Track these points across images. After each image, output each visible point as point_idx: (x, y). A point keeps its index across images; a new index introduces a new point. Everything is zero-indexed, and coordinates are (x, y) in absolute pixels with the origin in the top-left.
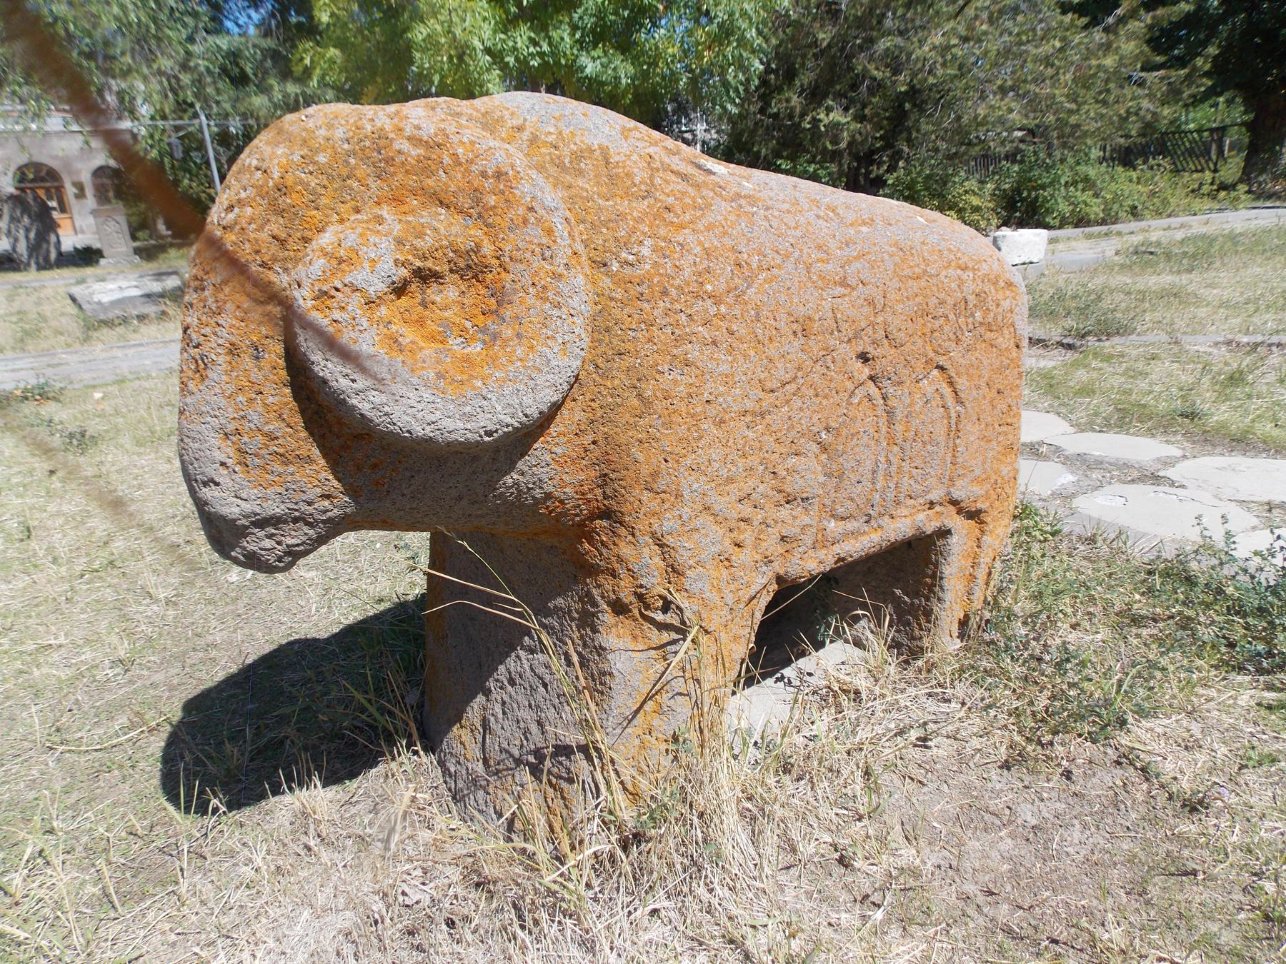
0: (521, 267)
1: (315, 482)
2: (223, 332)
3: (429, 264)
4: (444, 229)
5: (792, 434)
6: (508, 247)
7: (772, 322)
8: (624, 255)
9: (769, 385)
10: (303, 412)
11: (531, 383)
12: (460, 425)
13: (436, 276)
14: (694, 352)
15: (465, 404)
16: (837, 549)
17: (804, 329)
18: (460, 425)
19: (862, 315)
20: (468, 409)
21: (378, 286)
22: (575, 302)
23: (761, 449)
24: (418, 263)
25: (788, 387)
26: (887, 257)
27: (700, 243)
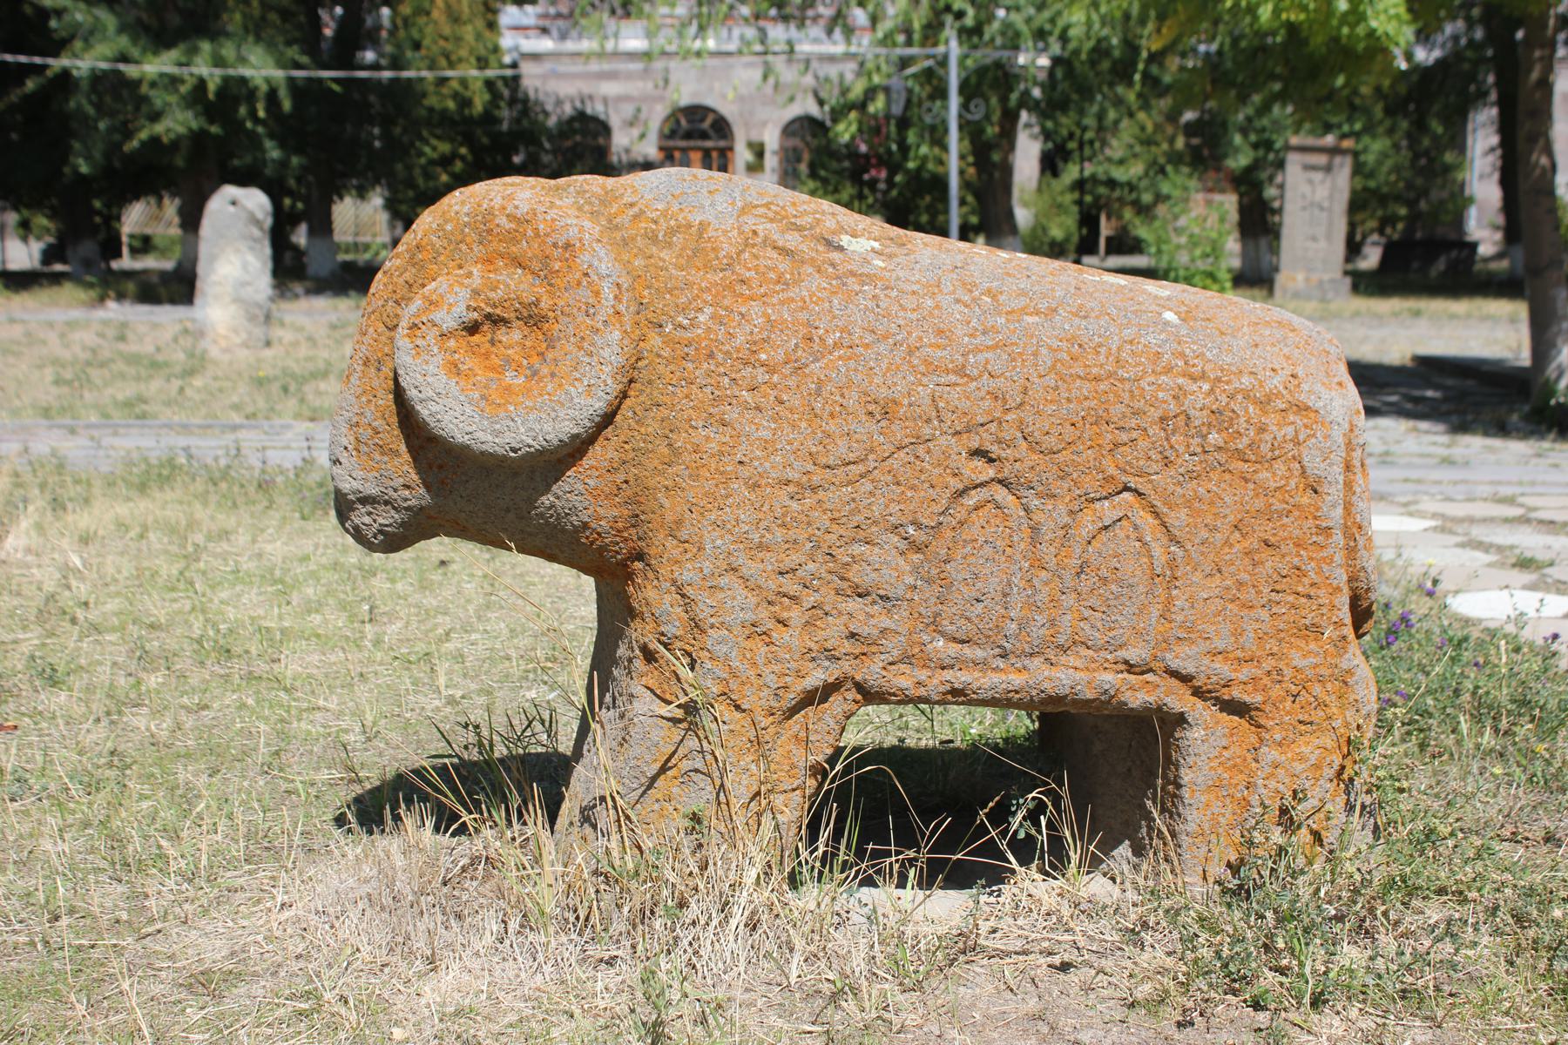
0: (567, 319)
1: (399, 475)
2: (363, 348)
3: (498, 311)
4: (514, 284)
6: (561, 303)
9: (824, 461)
10: (398, 414)
11: (553, 415)
12: (490, 438)
13: (505, 321)
14: (732, 414)
16: (948, 675)
17: (886, 411)
18: (490, 438)
19: (983, 409)
22: (606, 353)
23: (809, 524)
24: (489, 310)
26: (1044, 351)
27: (766, 315)
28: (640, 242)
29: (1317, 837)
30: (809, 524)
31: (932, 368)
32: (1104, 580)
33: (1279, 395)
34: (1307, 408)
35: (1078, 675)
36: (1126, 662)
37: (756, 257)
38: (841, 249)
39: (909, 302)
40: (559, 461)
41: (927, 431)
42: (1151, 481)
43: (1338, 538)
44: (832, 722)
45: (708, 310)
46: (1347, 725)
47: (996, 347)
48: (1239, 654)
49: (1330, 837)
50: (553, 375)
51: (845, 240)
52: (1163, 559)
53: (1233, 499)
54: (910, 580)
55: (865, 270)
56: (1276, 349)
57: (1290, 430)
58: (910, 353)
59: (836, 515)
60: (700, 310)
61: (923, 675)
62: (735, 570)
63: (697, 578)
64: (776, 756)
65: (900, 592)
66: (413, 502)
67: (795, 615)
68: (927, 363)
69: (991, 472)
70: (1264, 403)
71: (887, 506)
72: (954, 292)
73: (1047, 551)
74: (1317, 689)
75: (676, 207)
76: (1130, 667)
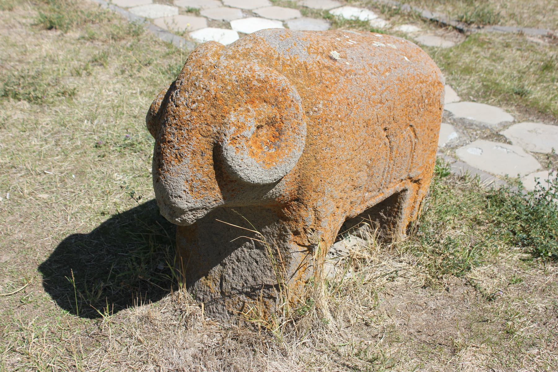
14: (334, 141)
20: (271, 173)
50: (286, 146)
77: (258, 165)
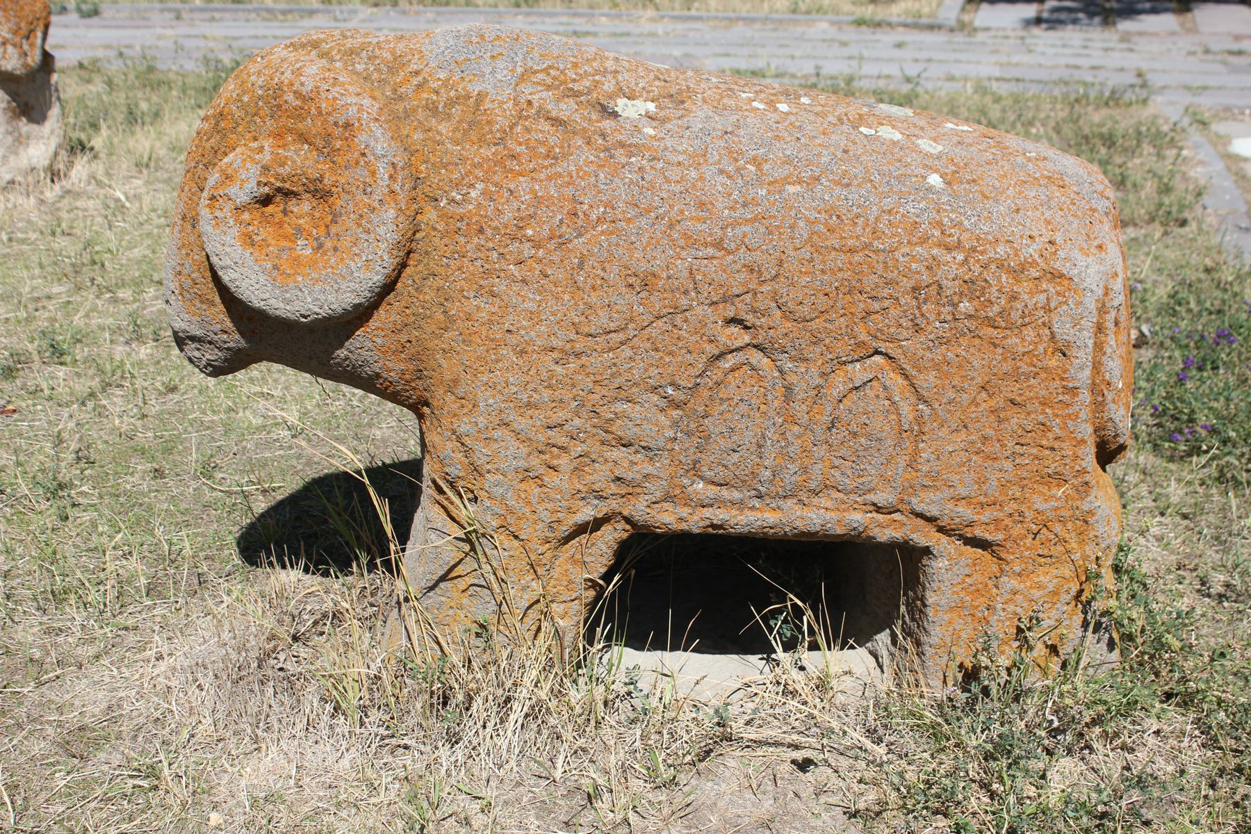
0: (347, 197)
3: (287, 186)
4: (300, 160)
5: (618, 381)
7: (599, 272)
8: (454, 194)
9: (586, 330)
11: (336, 286)
12: (282, 305)
13: (295, 194)
14: (501, 286)
15: (287, 292)
16: (707, 513)
17: (647, 283)
18: (282, 305)
21: (242, 198)
24: (279, 184)
25: (613, 335)
26: (801, 224)
27: (532, 191)
28: (421, 114)
29: (1053, 649)
30: (574, 386)
31: (691, 241)
32: (855, 434)
33: (1034, 263)
34: (1062, 276)
35: (829, 515)
36: (874, 504)
37: (528, 130)
38: (615, 115)
39: (674, 174)
40: (349, 322)
41: (684, 302)
42: (901, 347)
43: (1085, 396)
44: (604, 548)
45: (480, 186)
46: (1085, 558)
47: (754, 220)
48: (982, 499)
49: (1065, 650)
51: (621, 105)
52: (911, 417)
53: (980, 362)
54: (671, 434)
55: (634, 141)
56: (1038, 213)
57: (1043, 297)
58: (671, 226)
59: (599, 378)
60: (472, 186)
61: (684, 512)
62: (507, 425)
63: (473, 431)
64: (556, 573)
65: (661, 444)
66: (232, 345)
67: (564, 462)
68: (686, 236)
69: (747, 339)
70: (1017, 272)
71: (646, 370)
72: (719, 162)
73: (800, 409)
74: (1058, 528)
75: (456, 78)
76: (878, 509)
77: (256, 268)
